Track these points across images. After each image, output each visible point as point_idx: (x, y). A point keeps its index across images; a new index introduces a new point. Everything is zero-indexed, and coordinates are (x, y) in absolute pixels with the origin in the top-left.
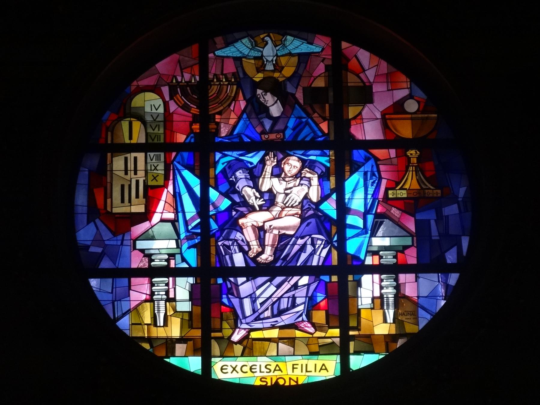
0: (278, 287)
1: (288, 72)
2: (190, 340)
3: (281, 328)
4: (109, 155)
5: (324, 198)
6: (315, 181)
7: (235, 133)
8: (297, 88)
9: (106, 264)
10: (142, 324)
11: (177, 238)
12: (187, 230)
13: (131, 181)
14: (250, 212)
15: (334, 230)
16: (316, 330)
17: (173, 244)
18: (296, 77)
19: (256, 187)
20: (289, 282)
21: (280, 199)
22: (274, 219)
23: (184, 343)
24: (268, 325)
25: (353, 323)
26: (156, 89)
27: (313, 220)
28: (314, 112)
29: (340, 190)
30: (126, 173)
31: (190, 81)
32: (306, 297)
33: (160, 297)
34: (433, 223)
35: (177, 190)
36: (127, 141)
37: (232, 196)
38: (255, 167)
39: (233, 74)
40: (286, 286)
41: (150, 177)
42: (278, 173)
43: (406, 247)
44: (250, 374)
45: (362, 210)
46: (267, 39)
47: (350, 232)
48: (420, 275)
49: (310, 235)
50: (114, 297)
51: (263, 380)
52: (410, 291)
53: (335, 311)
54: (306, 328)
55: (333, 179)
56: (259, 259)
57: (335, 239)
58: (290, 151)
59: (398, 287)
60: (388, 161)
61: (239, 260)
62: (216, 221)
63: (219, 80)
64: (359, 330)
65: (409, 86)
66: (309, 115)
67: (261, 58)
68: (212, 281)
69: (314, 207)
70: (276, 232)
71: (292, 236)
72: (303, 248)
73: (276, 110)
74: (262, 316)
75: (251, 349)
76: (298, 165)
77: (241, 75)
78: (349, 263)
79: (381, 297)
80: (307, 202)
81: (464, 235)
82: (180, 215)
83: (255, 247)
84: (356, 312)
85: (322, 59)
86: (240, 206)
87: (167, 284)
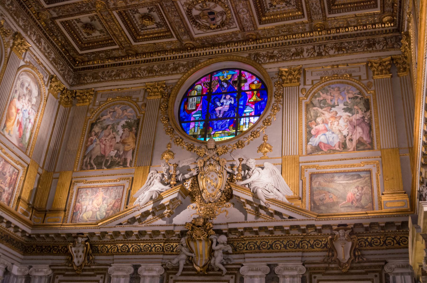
1: (229, 78)
9: (185, 120)
18: (231, 79)
19: (220, 102)
21: (225, 104)
25: (238, 129)
26: (200, 84)
42: (225, 98)
59: (249, 120)
73: (226, 86)
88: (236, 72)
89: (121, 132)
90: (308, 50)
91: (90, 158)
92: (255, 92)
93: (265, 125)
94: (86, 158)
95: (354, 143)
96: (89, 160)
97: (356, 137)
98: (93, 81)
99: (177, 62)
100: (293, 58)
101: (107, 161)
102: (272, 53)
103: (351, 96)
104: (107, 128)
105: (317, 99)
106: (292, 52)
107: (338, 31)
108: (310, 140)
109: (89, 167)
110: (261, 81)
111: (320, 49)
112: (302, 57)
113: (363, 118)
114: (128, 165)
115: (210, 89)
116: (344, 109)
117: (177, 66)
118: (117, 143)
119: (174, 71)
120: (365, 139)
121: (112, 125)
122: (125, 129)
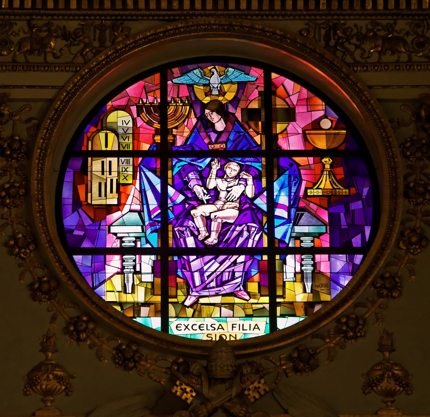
0: (221, 263)
1: (230, 96)
2: (152, 304)
3: (223, 295)
4: (90, 159)
5: (258, 195)
6: (250, 181)
7: (188, 143)
8: (236, 109)
9: (86, 244)
10: (115, 291)
11: (142, 225)
12: (150, 218)
13: (106, 180)
14: (200, 205)
15: (265, 220)
16: (250, 298)
17: (139, 229)
19: (204, 185)
20: (229, 260)
21: (223, 195)
22: (219, 210)
23: (148, 307)
24: (213, 293)
25: (279, 292)
26: (125, 108)
27: (248, 212)
28: (250, 127)
29: (270, 189)
30: (103, 174)
31: (153, 103)
32: (243, 272)
33: (129, 270)
34: (342, 215)
35: (143, 188)
36: (104, 149)
37: (185, 192)
38: (204, 170)
39: (187, 97)
40: (227, 263)
41: (122, 177)
42: (221, 174)
43: (321, 234)
44: (199, 331)
45: (287, 205)
46: (214, 70)
47: (277, 222)
48: (332, 255)
49: (246, 224)
50: (93, 270)
51: (209, 336)
52: (324, 268)
53: (266, 282)
54: (243, 296)
55: (264, 181)
56: (206, 241)
57: (266, 227)
58: (231, 158)
59: (314, 265)
60: (308, 167)
61: (191, 242)
62: (173, 212)
63: (175, 102)
64: (284, 298)
65: (324, 109)
67: (209, 85)
68: (170, 259)
69: (249, 202)
70: (219, 221)
71: (231, 224)
72: (241, 233)
73: (220, 126)
74: (208, 286)
75: (200, 311)
76: (238, 169)
77: (193, 99)
78: (277, 245)
79: (302, 272)
80: (244, 198)
81: (367, 225)
82: (145, 207)
83: (203, 233)
84: (281, 283)
85: (256, 86)
86: (191, 201)
87: (135, 261)
92: (327, 161)
93: (380, 296)
99: (39, 22)
102: (390, 28)
117: (44, 34)
119: (31, 52)
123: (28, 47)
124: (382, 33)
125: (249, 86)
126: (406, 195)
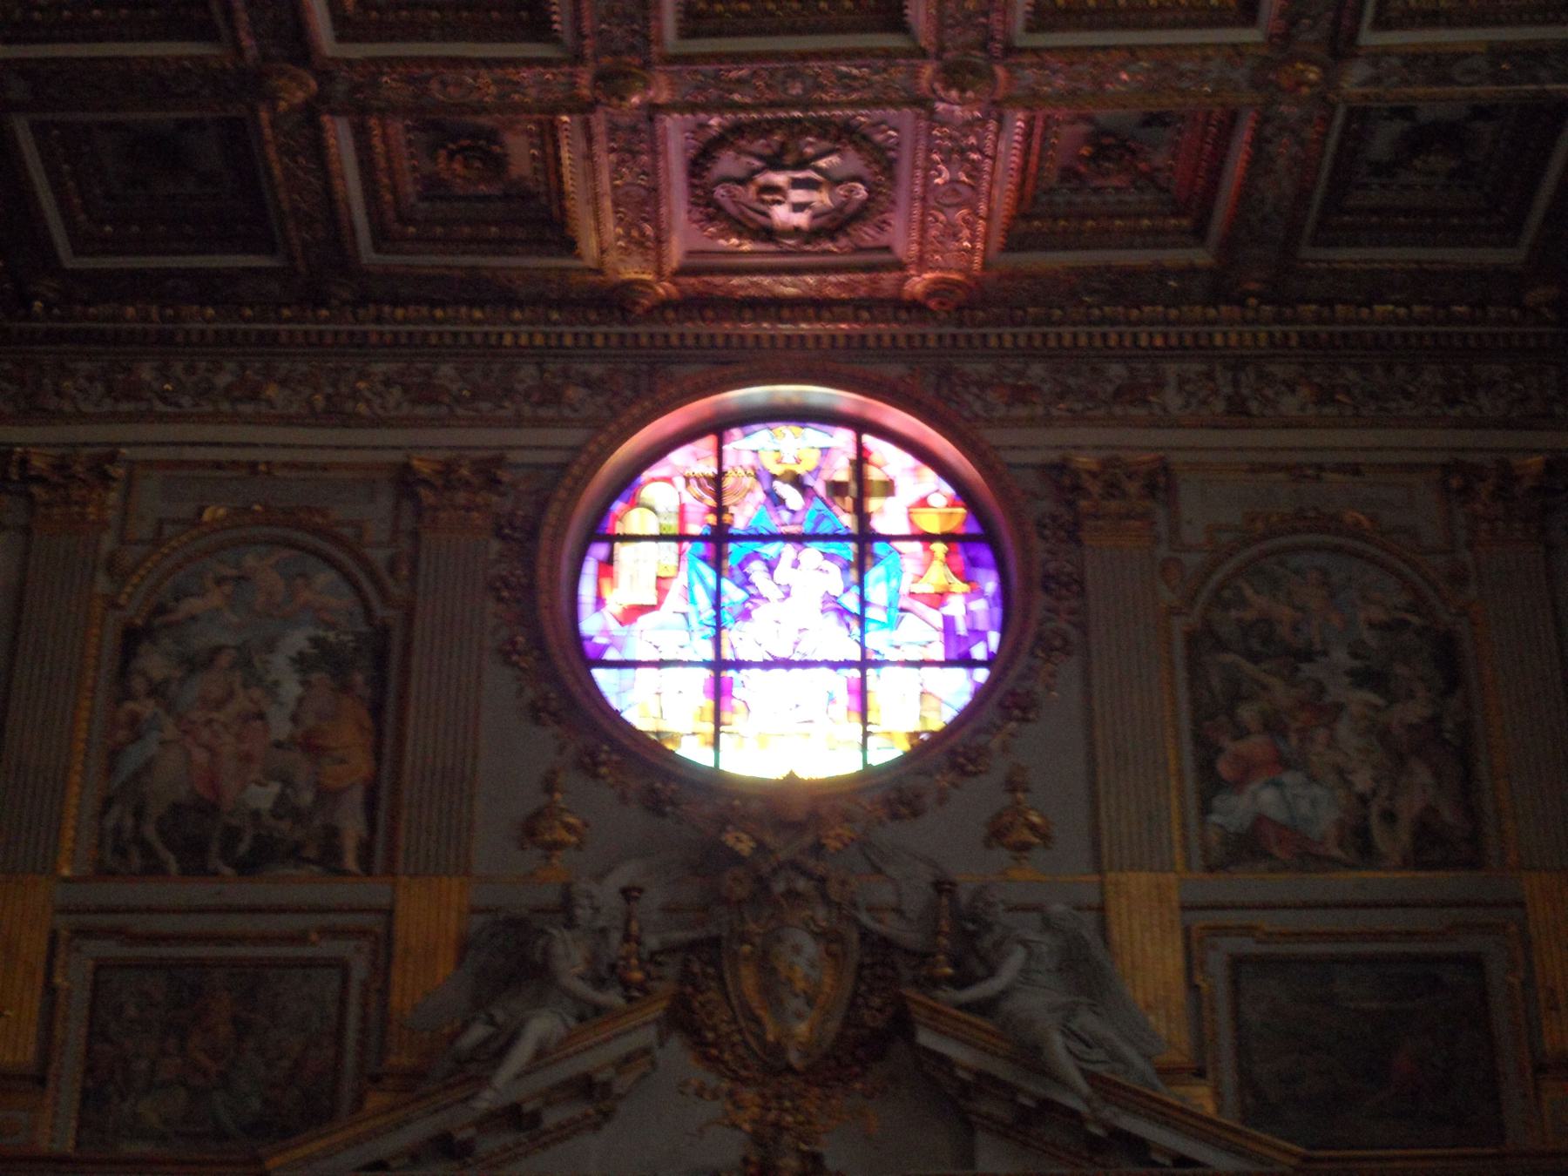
9: (611, 655)
26: (668, 480)
29: (861, 584)
53: (855, 704)
60: (913, 556)
66: (828, 507)
88: (843, 439)
89: (291, 688)
90: (1182, 382)
91: (139, 814)
92: (939, 548)
94: (116, 811)
95: (1405, 837)
96: (129, 822)
97: (1410, 806)
98: (107, 405)
99: (552, 367)
100: (1118, 410)
101: (233, 835)
102: (1020, 374)
103: (1377, 614)
104: (211, 660)
105: (1233, 613)
106: (1110, 381)
107: (1326, 312)
108: (1216, 802)
109: (136, 861)
110: (964, 493)
111: (1236, 383)
112: (1157, 411)
113: (1435, 720)
114: (350, 862)
115: (719, 510)
116: (1351, 673)
117: (558, 381)
118: (278, 745)
119: (541, 404)
120: (1447, 815)
121: (237, 648)
122: (315, 677)
123: (535, 397)
124: (1009, 380)
125: (834, 454)
126: (1046, 589)
